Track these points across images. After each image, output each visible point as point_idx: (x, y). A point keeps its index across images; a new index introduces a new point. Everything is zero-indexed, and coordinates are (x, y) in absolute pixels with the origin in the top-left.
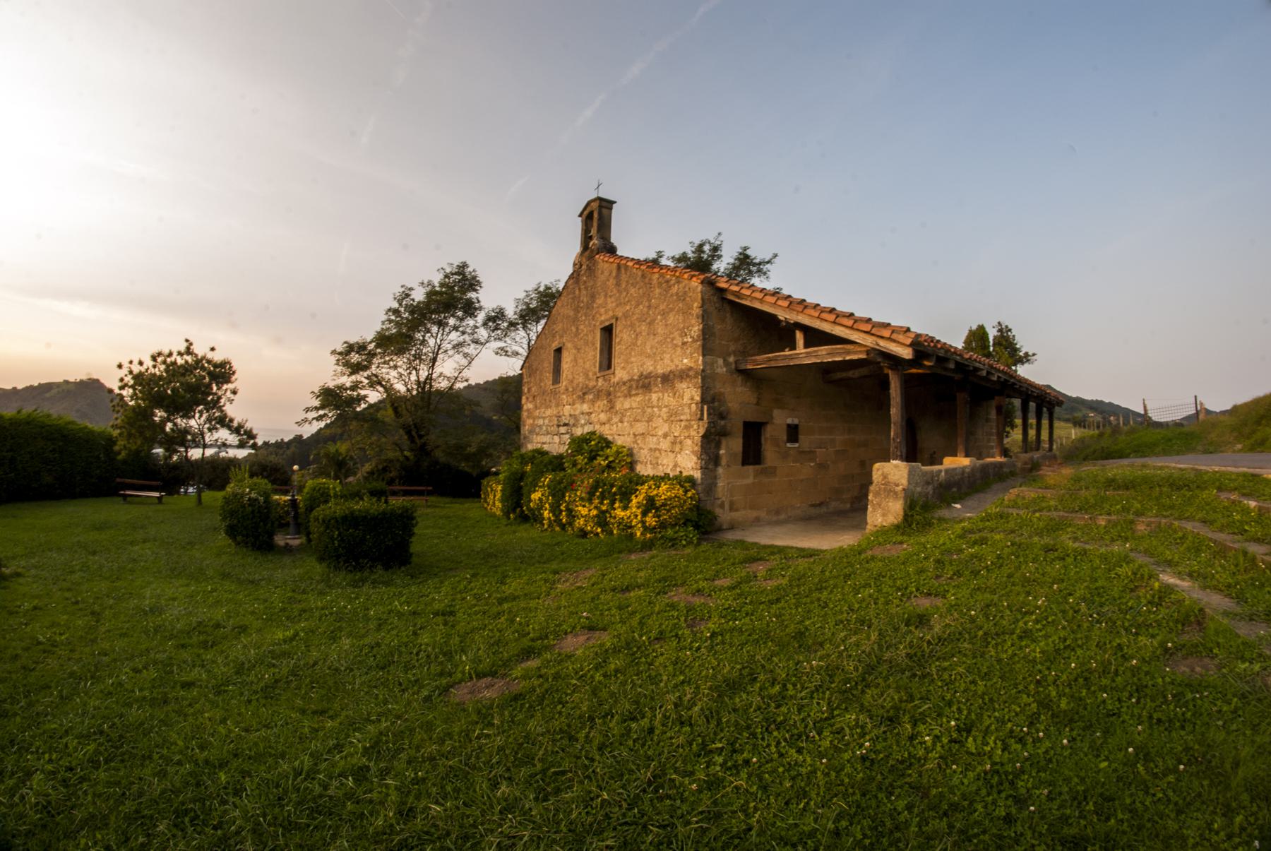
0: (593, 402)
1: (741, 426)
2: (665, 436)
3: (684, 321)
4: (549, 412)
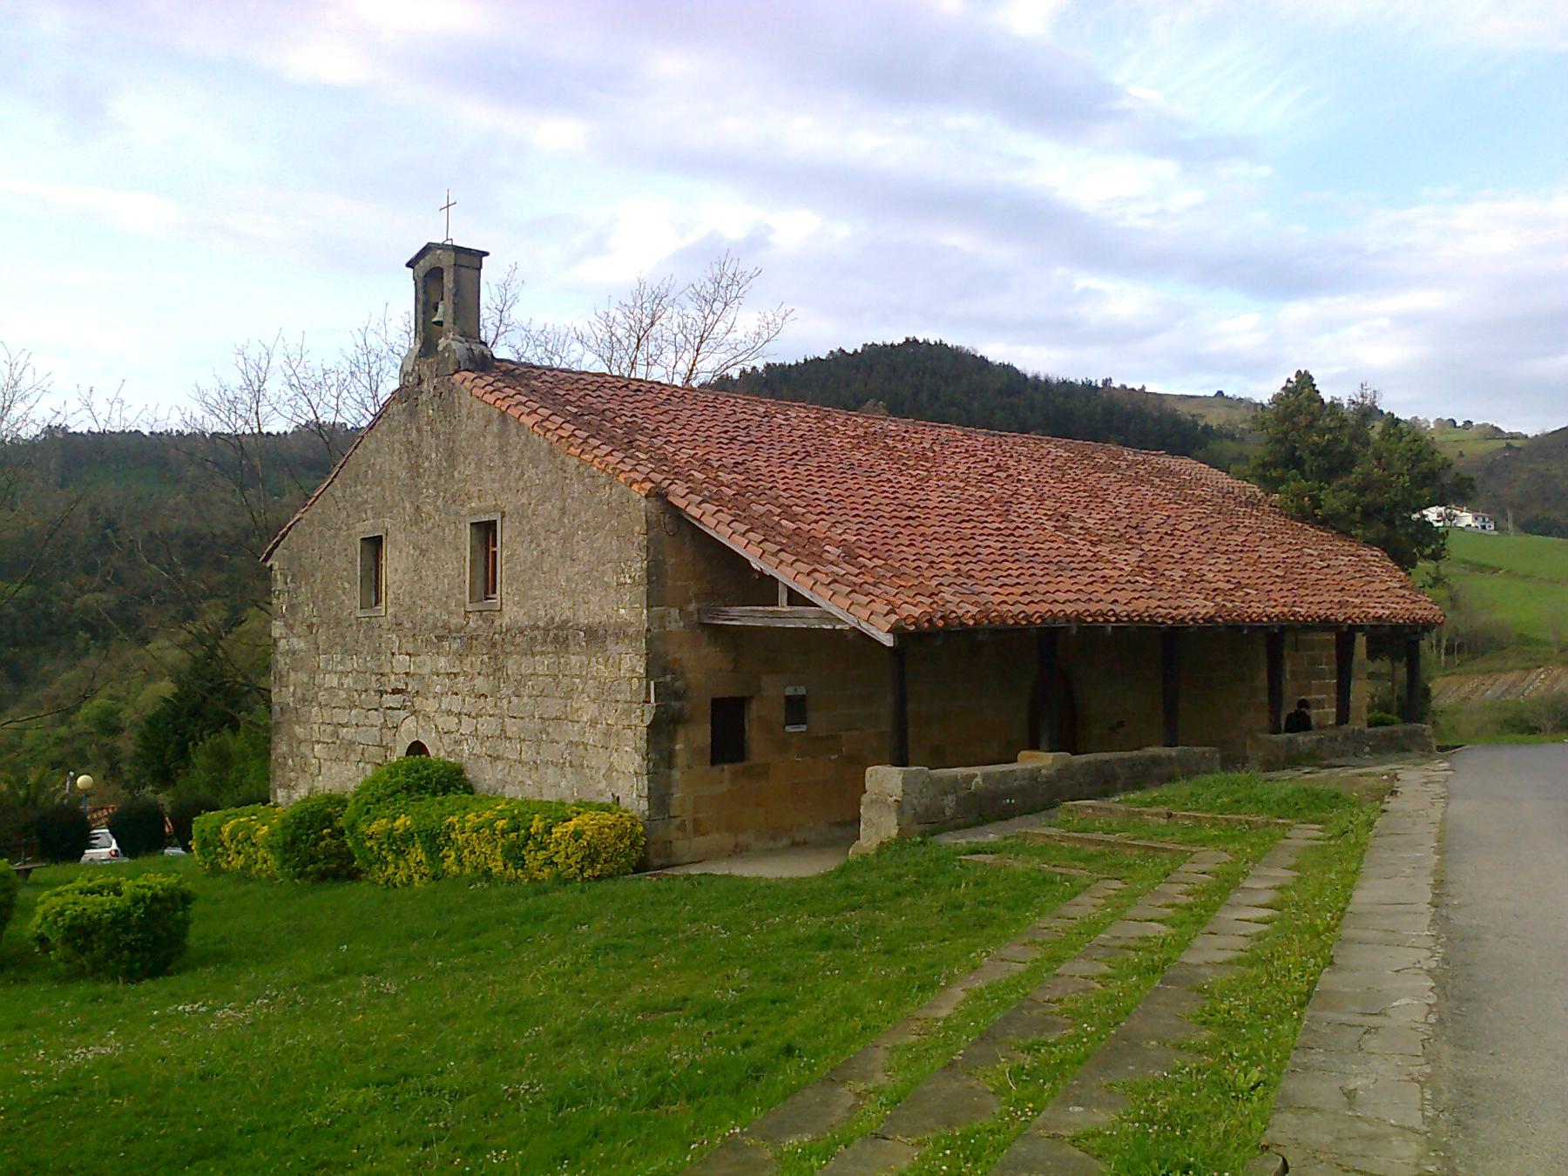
0: (460, 656)
1: (706, 709)
2: (593, 723)
4: (355, 663)
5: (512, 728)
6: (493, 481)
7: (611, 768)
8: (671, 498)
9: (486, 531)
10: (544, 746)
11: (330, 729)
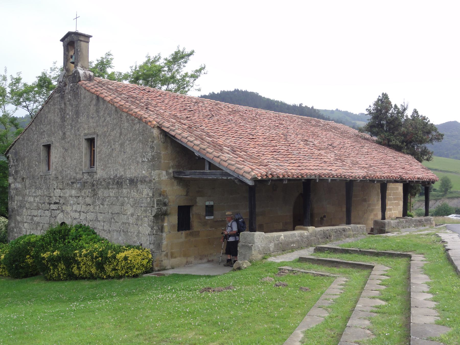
0: (80, 190)
2: (132, 215)
3: (143, 148)
4: (39, 192)
5: (100, 217)
6: (94, 123)
7: (139, 233)
8: (163, 128)
9: (91, 142)
10: (112, 224)
11: (30, 217)
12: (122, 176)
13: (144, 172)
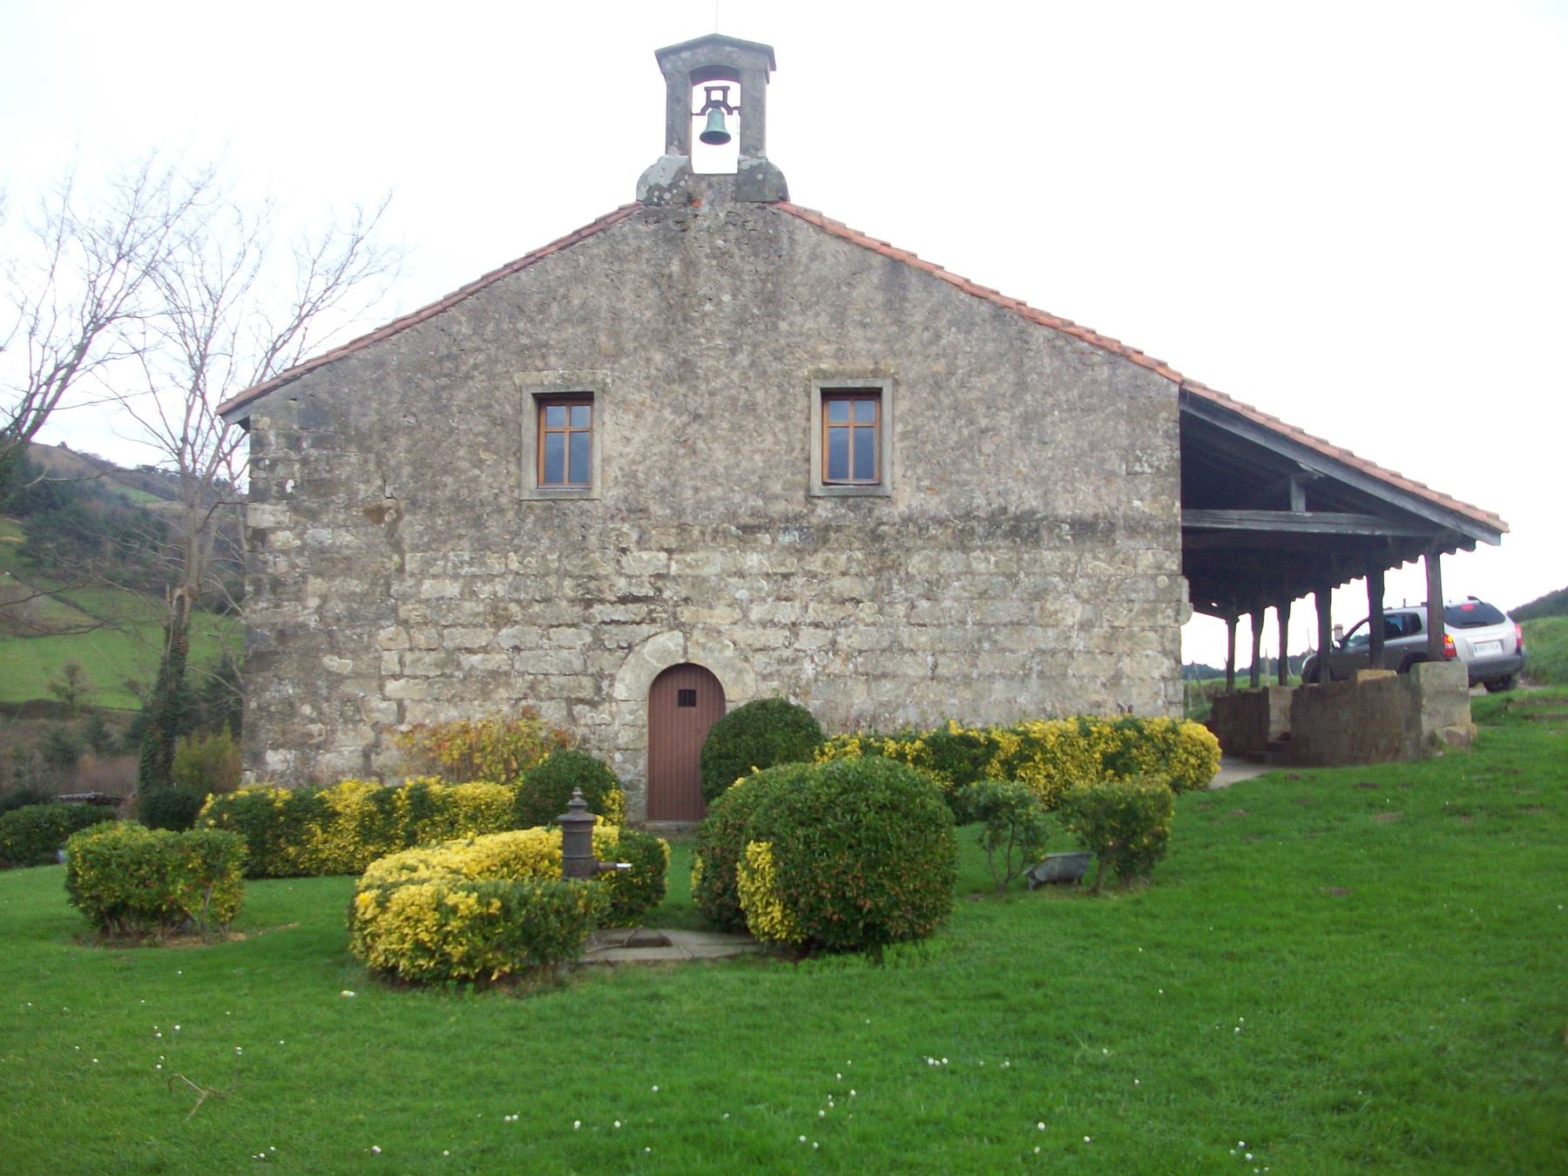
2: (1085, 626)
12: (1033, 512)
13: (1137, 503)
